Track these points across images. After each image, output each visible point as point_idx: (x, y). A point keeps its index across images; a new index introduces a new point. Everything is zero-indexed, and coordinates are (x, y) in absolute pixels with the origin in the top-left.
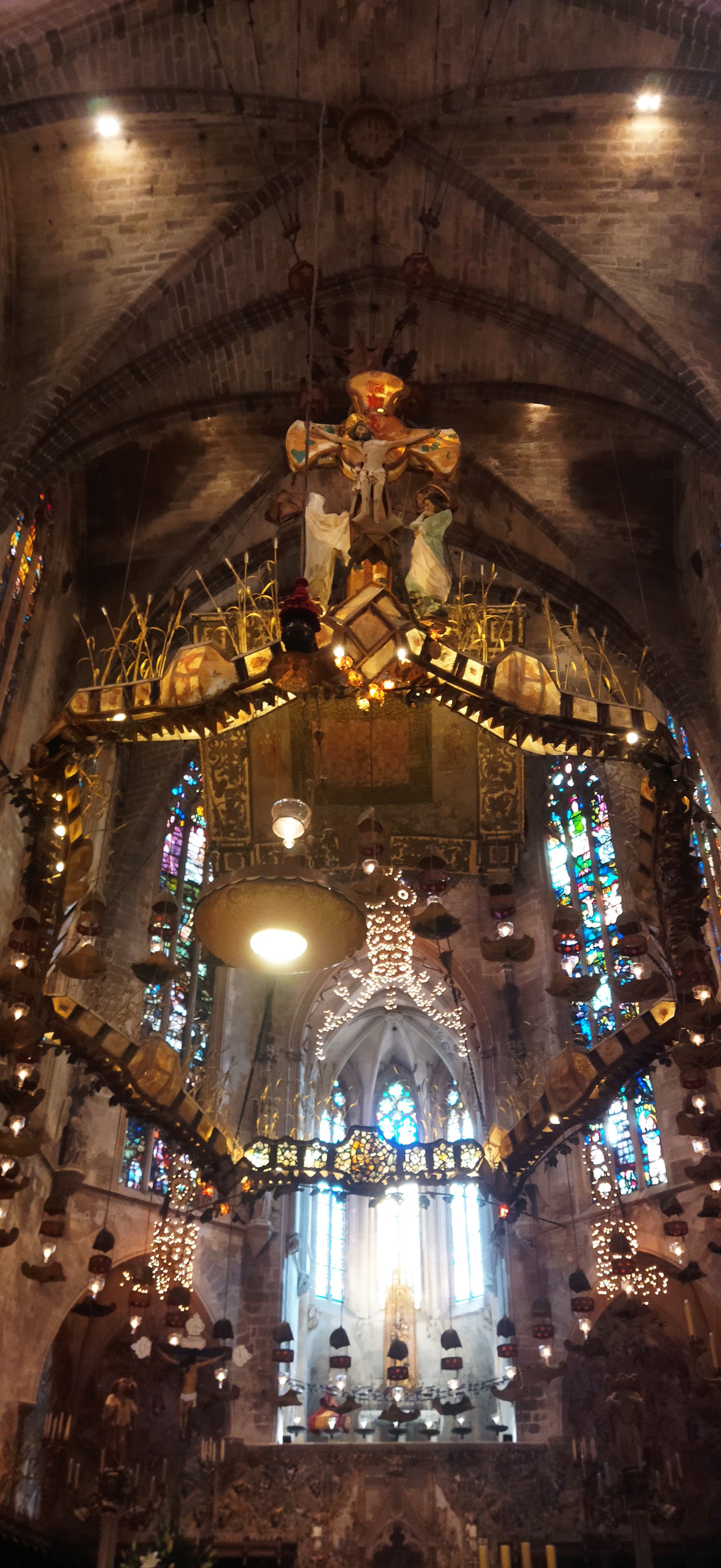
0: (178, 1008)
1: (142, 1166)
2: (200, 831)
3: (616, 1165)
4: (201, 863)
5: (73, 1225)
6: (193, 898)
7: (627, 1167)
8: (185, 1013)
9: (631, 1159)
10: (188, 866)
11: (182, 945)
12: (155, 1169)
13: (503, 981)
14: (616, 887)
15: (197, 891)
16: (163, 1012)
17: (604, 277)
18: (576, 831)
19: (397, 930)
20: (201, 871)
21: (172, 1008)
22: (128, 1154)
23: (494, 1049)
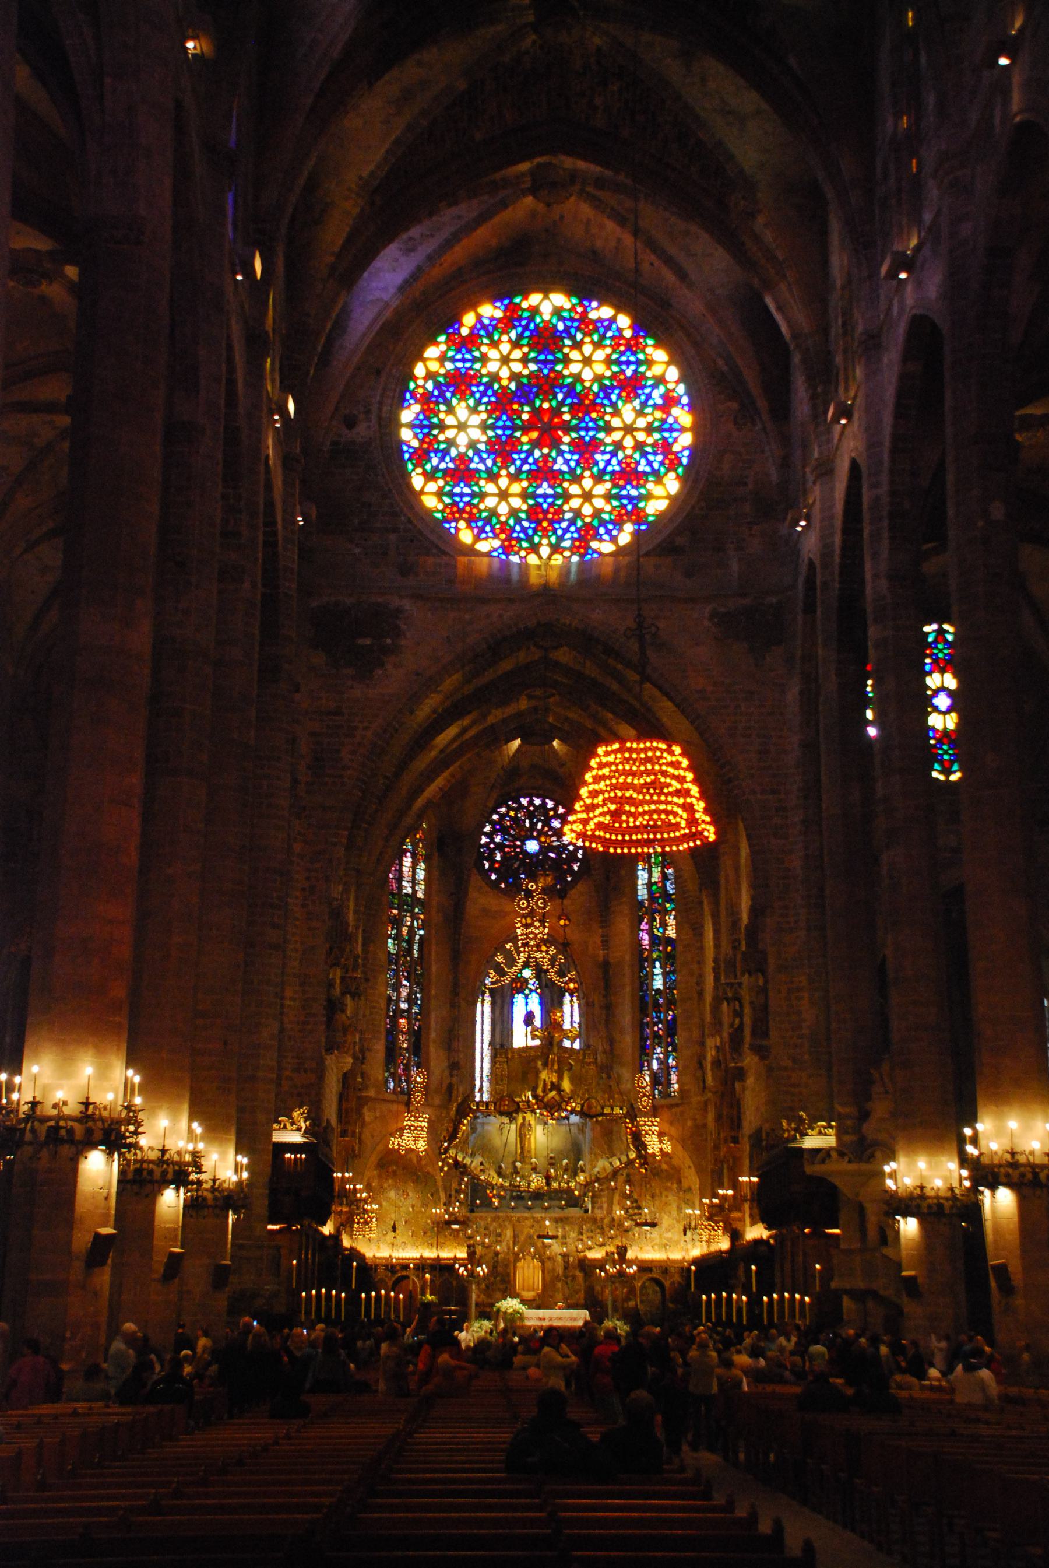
0: (405, 983)
1: (394, 1081)
2: (408, 854)
3: (656, 1080)
4: (410, 879)
5: (367, 1119)
6: (408, 906)
7: (660, 1084)
8: (408, 984)
9: (663, 1079)
10: (404, 883)
11: (404, 940)
12: (400, 1080)
13: (601, 959)
14: (673, 913)
15: (409, 899)
16: (397, 987)
17: (664, 720)
18: (655, 863)
19: (537, 931)
20: (411, 884)
21: (401, 983)
22: (386, 1074)
23: (593, 1002)
